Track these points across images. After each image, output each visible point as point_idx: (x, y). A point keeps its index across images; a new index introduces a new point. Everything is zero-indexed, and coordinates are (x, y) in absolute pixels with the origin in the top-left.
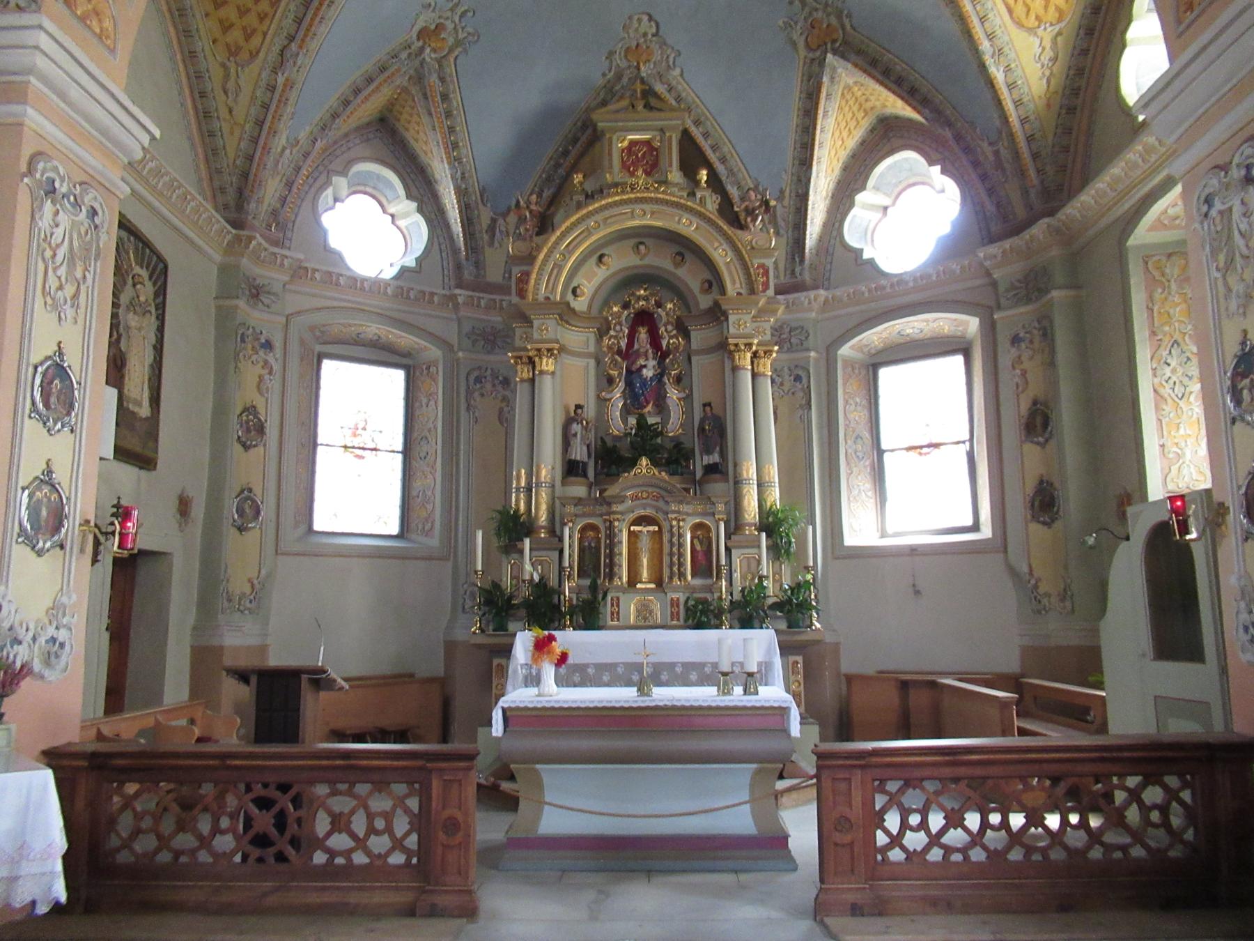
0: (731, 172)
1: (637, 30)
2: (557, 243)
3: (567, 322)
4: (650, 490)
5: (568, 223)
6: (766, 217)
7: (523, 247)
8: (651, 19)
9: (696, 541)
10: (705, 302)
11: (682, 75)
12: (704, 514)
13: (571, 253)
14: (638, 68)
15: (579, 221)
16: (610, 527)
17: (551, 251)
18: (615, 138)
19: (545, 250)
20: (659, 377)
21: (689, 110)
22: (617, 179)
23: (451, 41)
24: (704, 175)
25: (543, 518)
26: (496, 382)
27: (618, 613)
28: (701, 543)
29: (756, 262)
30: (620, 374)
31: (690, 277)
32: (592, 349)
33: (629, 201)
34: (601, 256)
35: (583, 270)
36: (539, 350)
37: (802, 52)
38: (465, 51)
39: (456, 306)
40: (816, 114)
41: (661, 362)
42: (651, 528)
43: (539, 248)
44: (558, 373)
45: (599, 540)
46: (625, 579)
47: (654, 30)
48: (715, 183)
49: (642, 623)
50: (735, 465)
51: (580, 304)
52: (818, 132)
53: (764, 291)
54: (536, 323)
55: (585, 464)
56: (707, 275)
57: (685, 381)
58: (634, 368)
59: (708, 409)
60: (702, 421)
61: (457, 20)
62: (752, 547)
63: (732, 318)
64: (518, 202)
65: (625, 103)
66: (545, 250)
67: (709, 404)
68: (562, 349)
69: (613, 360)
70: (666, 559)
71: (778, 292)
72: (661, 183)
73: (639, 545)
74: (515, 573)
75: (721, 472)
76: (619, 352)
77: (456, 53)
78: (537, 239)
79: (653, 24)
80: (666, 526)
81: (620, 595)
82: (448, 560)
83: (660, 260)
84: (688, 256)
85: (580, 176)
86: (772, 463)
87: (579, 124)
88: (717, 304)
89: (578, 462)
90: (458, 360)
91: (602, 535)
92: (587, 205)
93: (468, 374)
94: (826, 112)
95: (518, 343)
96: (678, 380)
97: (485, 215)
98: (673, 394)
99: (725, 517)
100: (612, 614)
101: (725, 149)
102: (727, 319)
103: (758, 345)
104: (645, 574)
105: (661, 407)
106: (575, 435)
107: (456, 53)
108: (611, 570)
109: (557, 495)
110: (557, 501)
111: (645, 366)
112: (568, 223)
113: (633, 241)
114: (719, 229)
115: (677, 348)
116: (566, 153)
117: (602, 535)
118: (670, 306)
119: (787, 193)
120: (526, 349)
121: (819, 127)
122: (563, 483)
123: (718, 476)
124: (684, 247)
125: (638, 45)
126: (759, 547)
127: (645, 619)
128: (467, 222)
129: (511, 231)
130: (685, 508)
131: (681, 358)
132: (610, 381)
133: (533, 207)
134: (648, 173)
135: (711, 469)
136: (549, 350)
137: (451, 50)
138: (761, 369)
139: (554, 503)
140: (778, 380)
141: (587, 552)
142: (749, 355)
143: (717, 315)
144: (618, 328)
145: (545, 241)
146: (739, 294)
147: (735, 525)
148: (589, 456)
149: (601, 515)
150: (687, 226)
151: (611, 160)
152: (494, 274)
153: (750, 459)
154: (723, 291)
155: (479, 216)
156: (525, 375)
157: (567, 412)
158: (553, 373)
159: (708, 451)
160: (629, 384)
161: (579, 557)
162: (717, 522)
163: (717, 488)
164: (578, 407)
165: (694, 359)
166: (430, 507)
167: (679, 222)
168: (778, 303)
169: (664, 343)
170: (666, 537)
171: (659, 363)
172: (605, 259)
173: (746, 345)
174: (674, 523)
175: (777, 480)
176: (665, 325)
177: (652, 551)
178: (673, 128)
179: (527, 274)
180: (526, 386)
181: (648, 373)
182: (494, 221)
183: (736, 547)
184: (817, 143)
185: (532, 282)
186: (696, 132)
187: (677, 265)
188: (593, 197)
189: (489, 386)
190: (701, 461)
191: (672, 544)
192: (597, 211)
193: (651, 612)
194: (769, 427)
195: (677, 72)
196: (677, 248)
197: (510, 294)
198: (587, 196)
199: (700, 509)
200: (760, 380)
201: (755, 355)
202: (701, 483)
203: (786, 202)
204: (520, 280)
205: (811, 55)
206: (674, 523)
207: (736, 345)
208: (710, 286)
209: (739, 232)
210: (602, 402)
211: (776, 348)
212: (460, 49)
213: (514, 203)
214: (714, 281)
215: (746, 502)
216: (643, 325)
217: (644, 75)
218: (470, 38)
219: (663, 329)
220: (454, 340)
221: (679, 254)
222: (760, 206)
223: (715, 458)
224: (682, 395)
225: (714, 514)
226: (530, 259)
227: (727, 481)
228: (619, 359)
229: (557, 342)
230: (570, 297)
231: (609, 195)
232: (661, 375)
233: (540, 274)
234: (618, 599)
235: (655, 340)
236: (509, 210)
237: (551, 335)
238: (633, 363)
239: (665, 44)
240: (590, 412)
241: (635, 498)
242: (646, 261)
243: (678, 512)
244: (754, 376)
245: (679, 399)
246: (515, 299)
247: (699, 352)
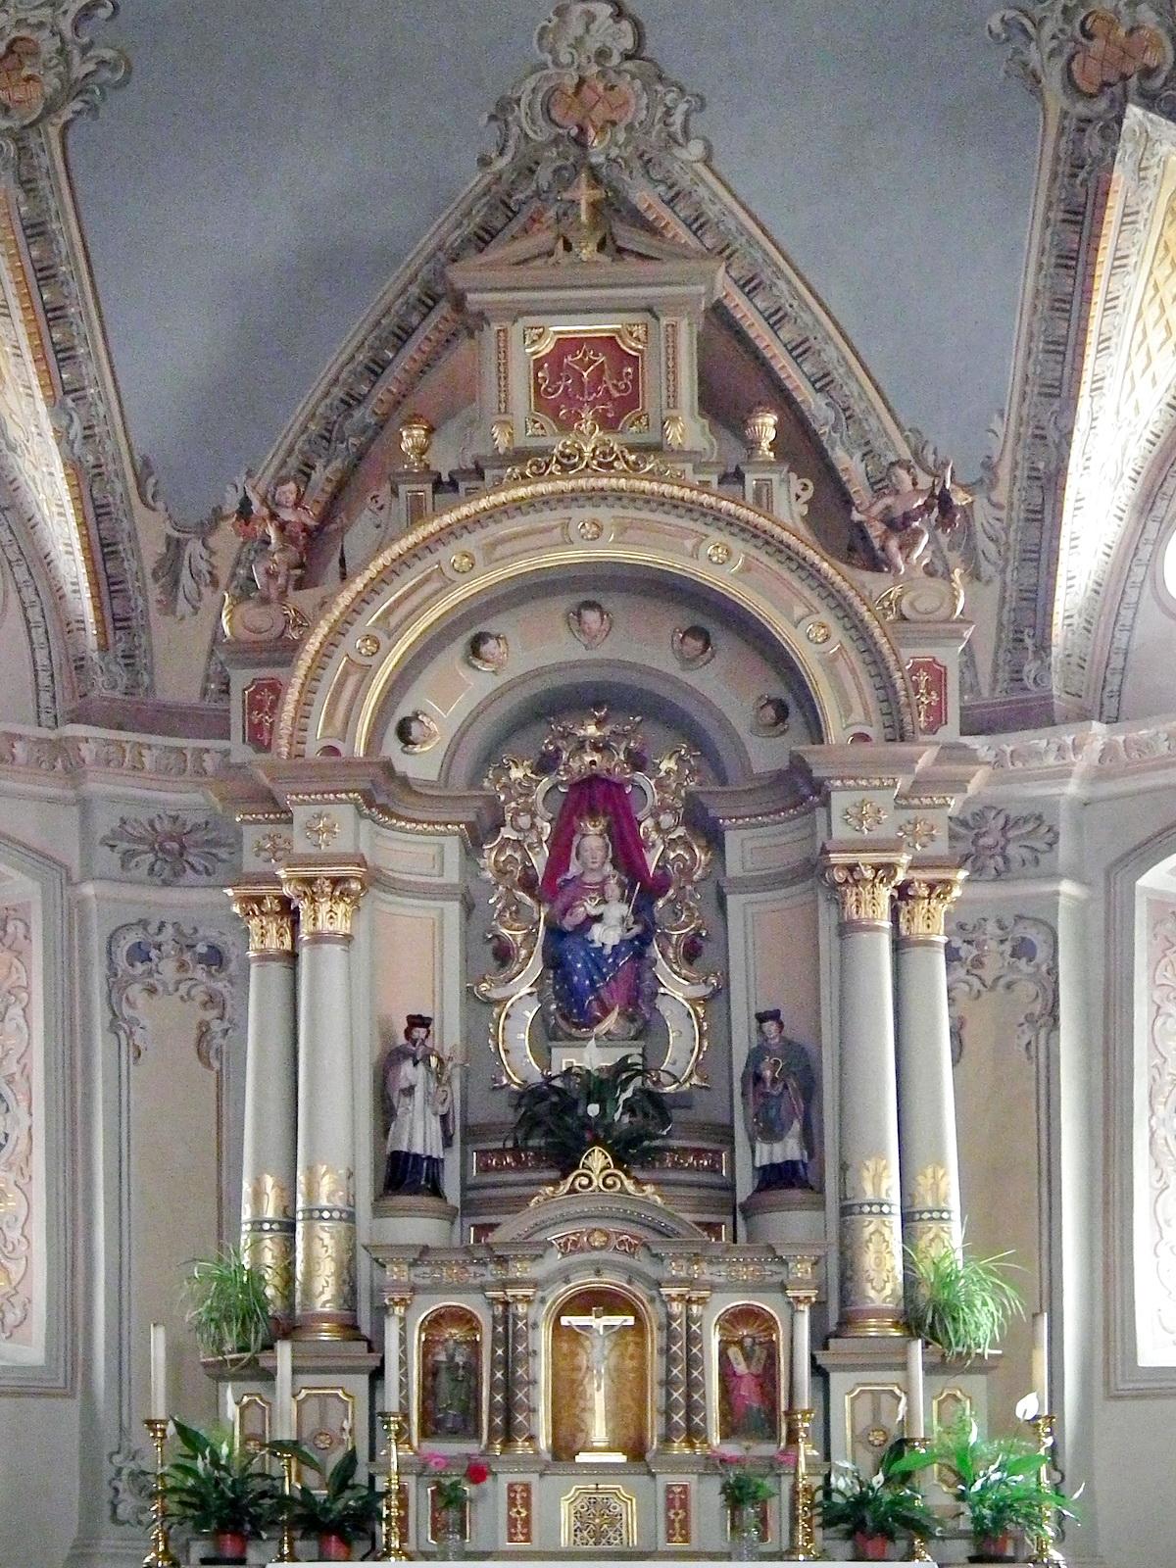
0: (847, 413)
1: (578, 42)
2: (355, 610)
3: (385, 810)
4: (613, 1227)
5: (384, 559)
6: (944, 539)
7: (262, 620)
8: (619, 14)
9: (734, 1352)
10: (766, 755)
11: (707, 161)
12: (760, 1287)
13: (394, 634)
14: (580, 141)
15: (415, 554)
16: (505, 1317)
17: (338, 631)
18: (516, 331)
19: (323, 628)
20: (637, 947)
21: (724, 252)
22: (521, 442)
23: (51, 82)
24: (767, 426)
25: (325, 1294)
26: (187, 956)
27: (527, 1522)
28: (748, 1358)
29: (909, 655)
30: (531, 936)
31: (725, 689)
32: (452, 876)
33: (561, 499)
34: (475, 646)
35: (429, 676)
36: (309, 882)
37: (1055, 97)
38: (93, 109)
39: (74, 771)
40: (1091, 264)
41: (642, 908)
42: (617, 1320)
43: (303, 622)
44: (362, 940)
45: (476, 1346)
46: (544, 1442)
47: (628, 43)
48: (803, 446)
49: (591, 1547)
50: (844, 1168)
51: (421, 764)
52: (1096, 311)
53: (932, 729)
54: (301, 814)
55: (435, 1163)
56: (778, 690)
57: (708, 949)
58: (569, 923)
59: (770, 1027)
60: (756, 1056)
61: (66, 25)
62: (890, 1367)
63: (840, 801)
64: (246, 503)
65: (543, 238)
66: (323, 628)
67: (775, 1016)
68: (375, 879)
69: (512, 902)
70: (655, 1396)
71: (974, 725)
72: (645, 449)
73: (583, 1360)
74: (254, 1427)
75: (805, 1185)
76: (528, 883)
77: (67, 114)
78: (304, 599)
79: (626, 25)
80: (654, 1315)
81: (533, 1478)
82: (73, 1396)
83: (644, 647)
84: (726, 643)
85: (418, 433)
86: (939, 1161)
87: (415, 290)
88: (798, 767)
89: (416, 1156)
90: (82, 902)
91: (486, 1338)
92: (437, 513)
93: (112, 939)
94: (1119, 261)
95: (251, 863)
96: (692, 951)
97: (150, 533)
98: (677, 991)
99: (812, 1293)
100: (512, 1522)
101: (830, 354)
102: (826, 803)
103: (912, 867)
104: (599, 1430)
105: (645, 1025)
106: (409, 1091)
107: (67, 114)
108: (508, 1420)
109: (363, 1237)
110: (364, 1261)
111: (598, 919)
112: (384, 559)
113: (565, 603)
114: (811, 573)
115: (687, 872)
116: (376, 369)
117: (486, 1338)
118: (668, 764)
119: (1004, 472)
120: (278, 882)
121: (1098, 298)
122: (378, 1211)
123: (796, 1194)
124: (712, 617)
125: (582, 81)
126: (904, 1366)
127: (598, 1536)
128: (103, 551)
129: (223, 576)
130: (703, 1271)
131: (699, 899)
132: (503, 954)
133: (287, 515)
134: (608, 424)
135: (778, 1177)
136: (336, 881)
137: (50, 109)
138: (919, 928)
139: (353, 1259)
140: (966, 951)
141: (444, 1377)
142: (885, 893)
143: (800, 790)
144: (524, 821)
145: (324, 605)
146: (862, 738)
147: (838, 1317)
148: (447, 1141)
149: (482, 1288)
150: (718, 564)
151: (504, 388)
152: (178, 677)
153: (880, 1152)
154: (816, 730)
155: (133, 536)
156: (273, 943)
157: (386, 1035)
158: (348, 939)
159: (769, 1129)
160: (555, 962)
161: (423, 1387)
162: (793, 1305)
163: (793, 1223)
164: (417, 1021)
165: (732, 901)
166: (16, 1270)
167: (694, 555)
168: (971, 758)
169: (652, 860)
170: (655, 1340)
171: (636, 912)
172: (489, 647)
173: (876, 868)
174: (677, 1308)
175: (954, 1203)
176: (655, 814)
177: (617, 1374)
178: (677, 306)
179: (276, 689)
180: (277, 971)
181: (606, 936)
182: (175, 546)
183: (843, 1368)
184: (1092, 338)
185: (288, 710)
186: (747, 314)
187: (688, 662)
188: (453, 485)
189: (168, 969)
190: (749, 1158)
191: (671, 1360)
192: (466, 525)
193: (614, 1520)
194: (937, 1075)
195: (696, 149)
196: (685, 618)
197: (226, 735)
198: (438, 485)
199: (745, 1273)
200: (914, 955)
201: (903, 892)
202: (749, 1210)
203: (1001, 494)
204: (254, 704)
205: (1081, 108)
206: (677, 1308)
207: (851, 868)
208: (782, 711)
209: (867, 577)
210: (479, 1005)
211: (962, 874)
212: (77, 105)
213: (232, 504)
214: (792, 703)
215: (869, 1260)
216: (593, 814)
217: (597, 159)
218: (106, 74)
219: (649, 823)
220: (70, 853)
221: (696, 632)
222: (927, 507)
223: (789, 1149)
224: (702, 991)
225: (783, 1287)
226: (284, 650)
227: (821, 1206)
228: (528, 900)
229: (362, 863)
230: (392, 747)
231: (499, 485)
232: (644, 939)
233: (308, 690)
234: (527, 1488)
235: (626, 850)
236: (218, 516)
237: (343, 844)
238: (567, 909)
239: (660, 78)
240: (449, 1035)
241: (570, 1247)
242: (604, 651)
243: (691, 1283)
244: (899, 945)
245: (693, 1001)
246: (240, 750)
247: (745, 885)
